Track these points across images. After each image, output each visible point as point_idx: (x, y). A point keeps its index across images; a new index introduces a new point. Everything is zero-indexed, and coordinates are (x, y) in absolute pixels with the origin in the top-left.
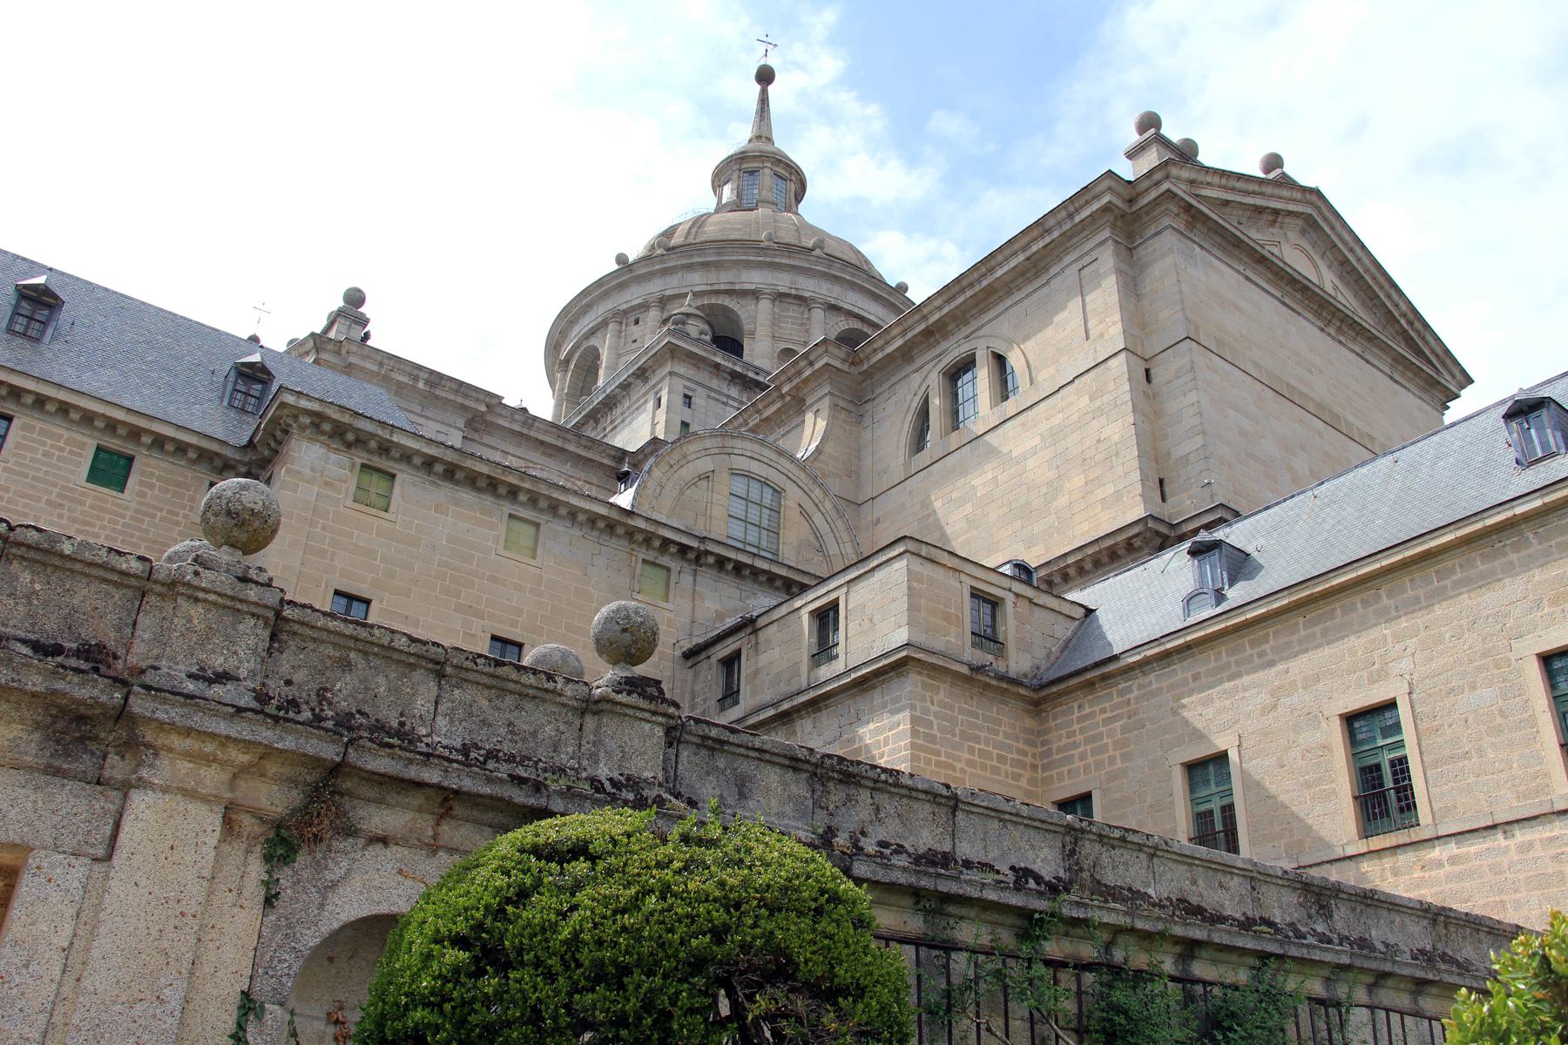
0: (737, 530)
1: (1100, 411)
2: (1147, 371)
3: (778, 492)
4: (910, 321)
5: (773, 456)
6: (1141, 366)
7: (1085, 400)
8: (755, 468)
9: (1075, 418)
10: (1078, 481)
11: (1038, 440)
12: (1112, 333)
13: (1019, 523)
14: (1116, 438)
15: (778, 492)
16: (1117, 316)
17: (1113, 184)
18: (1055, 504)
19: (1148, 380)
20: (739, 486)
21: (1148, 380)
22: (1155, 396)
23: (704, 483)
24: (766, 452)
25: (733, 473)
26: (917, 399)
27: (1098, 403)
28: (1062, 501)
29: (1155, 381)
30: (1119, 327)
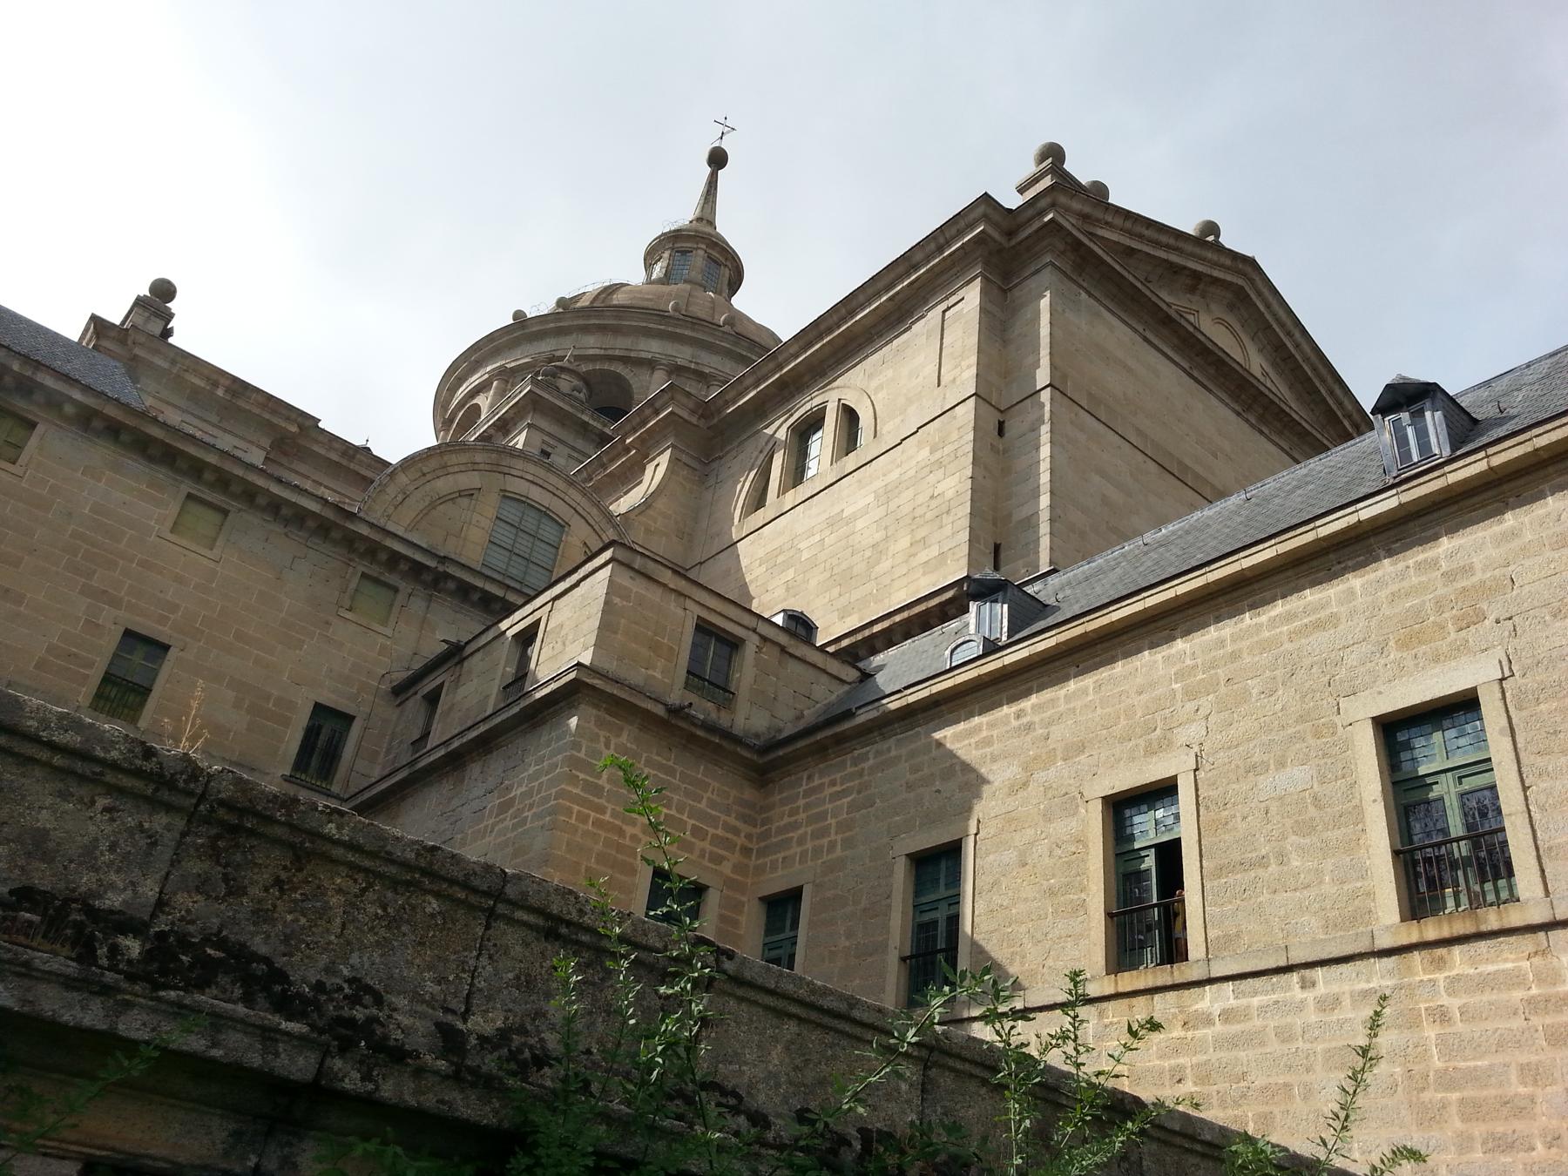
0: (499, 560)
1: (939, 464)
2: (1001, 425)
3: (562, 526)
4: (765, 370)
5: (562, 485)
6: (994, 417)
7: (925, 452)
8: (536, 494)
9: (912, 472)
10: (904, 542)
11: (871, 498)
12: (964, 375)
13: (836, 591)
14: (950, 494)
15: (562, 526)
16: (974, 359)
17: (990, 211)
18: (877, 569)
19: (1001, 432)
20: (512, 512)
21: (1001, 432)
22: (1005, 451)
23: (465, 502)
24: (553, 479)
25: (506, 496)
26: (762, 457)
27: (938, 455)
28: (885, 565)
29: (1010, 432)
30: (974, 370)
